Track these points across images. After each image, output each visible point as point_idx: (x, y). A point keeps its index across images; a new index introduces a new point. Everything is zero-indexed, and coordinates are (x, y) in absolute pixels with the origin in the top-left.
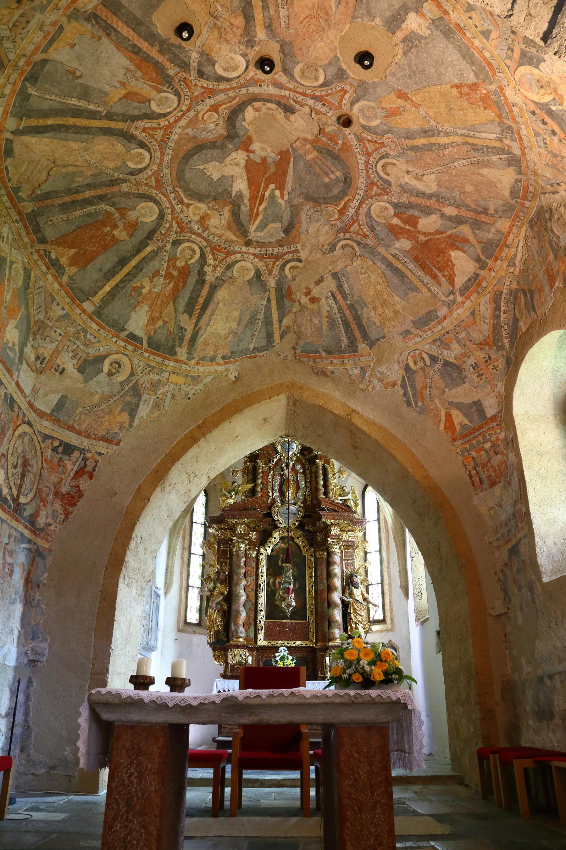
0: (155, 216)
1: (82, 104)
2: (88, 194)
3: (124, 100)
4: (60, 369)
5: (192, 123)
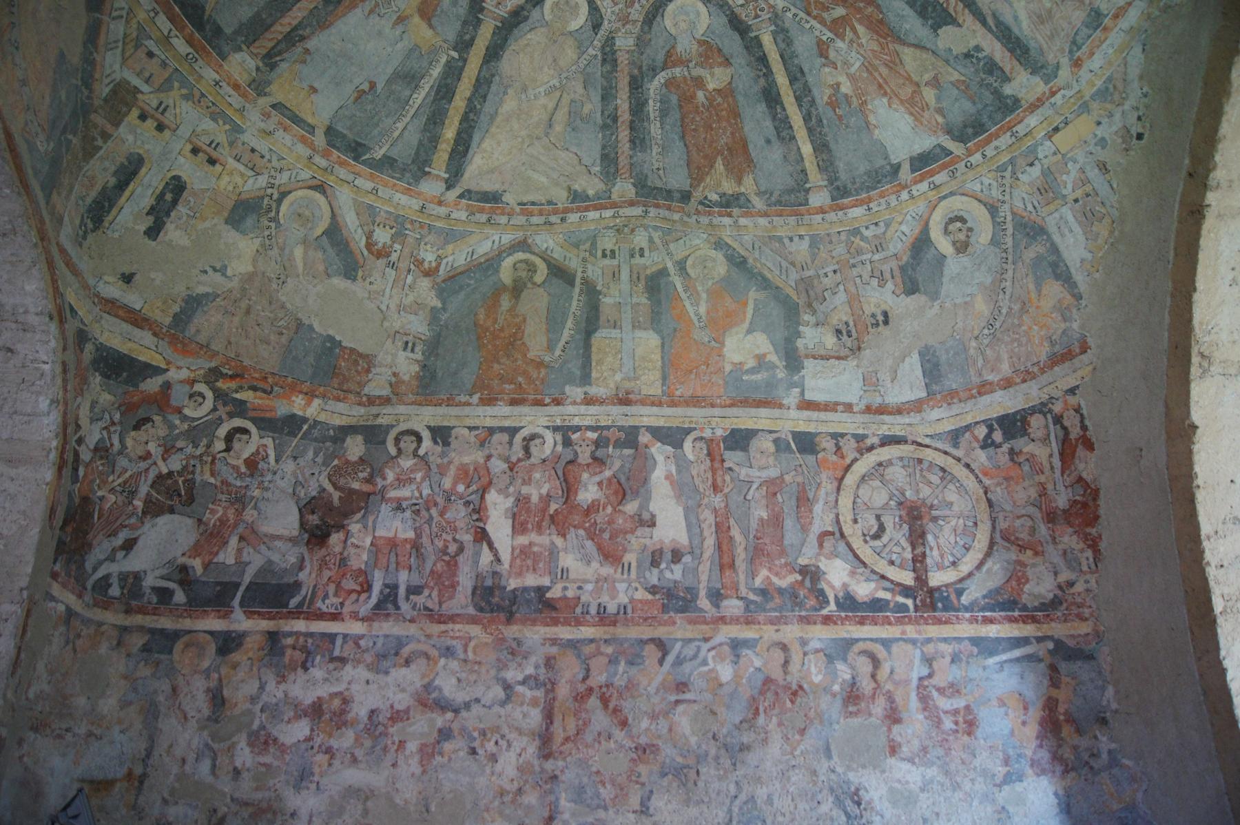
1: (426, 86)
2: (623, 102)
3: (434, 21)
4: (881, 318)
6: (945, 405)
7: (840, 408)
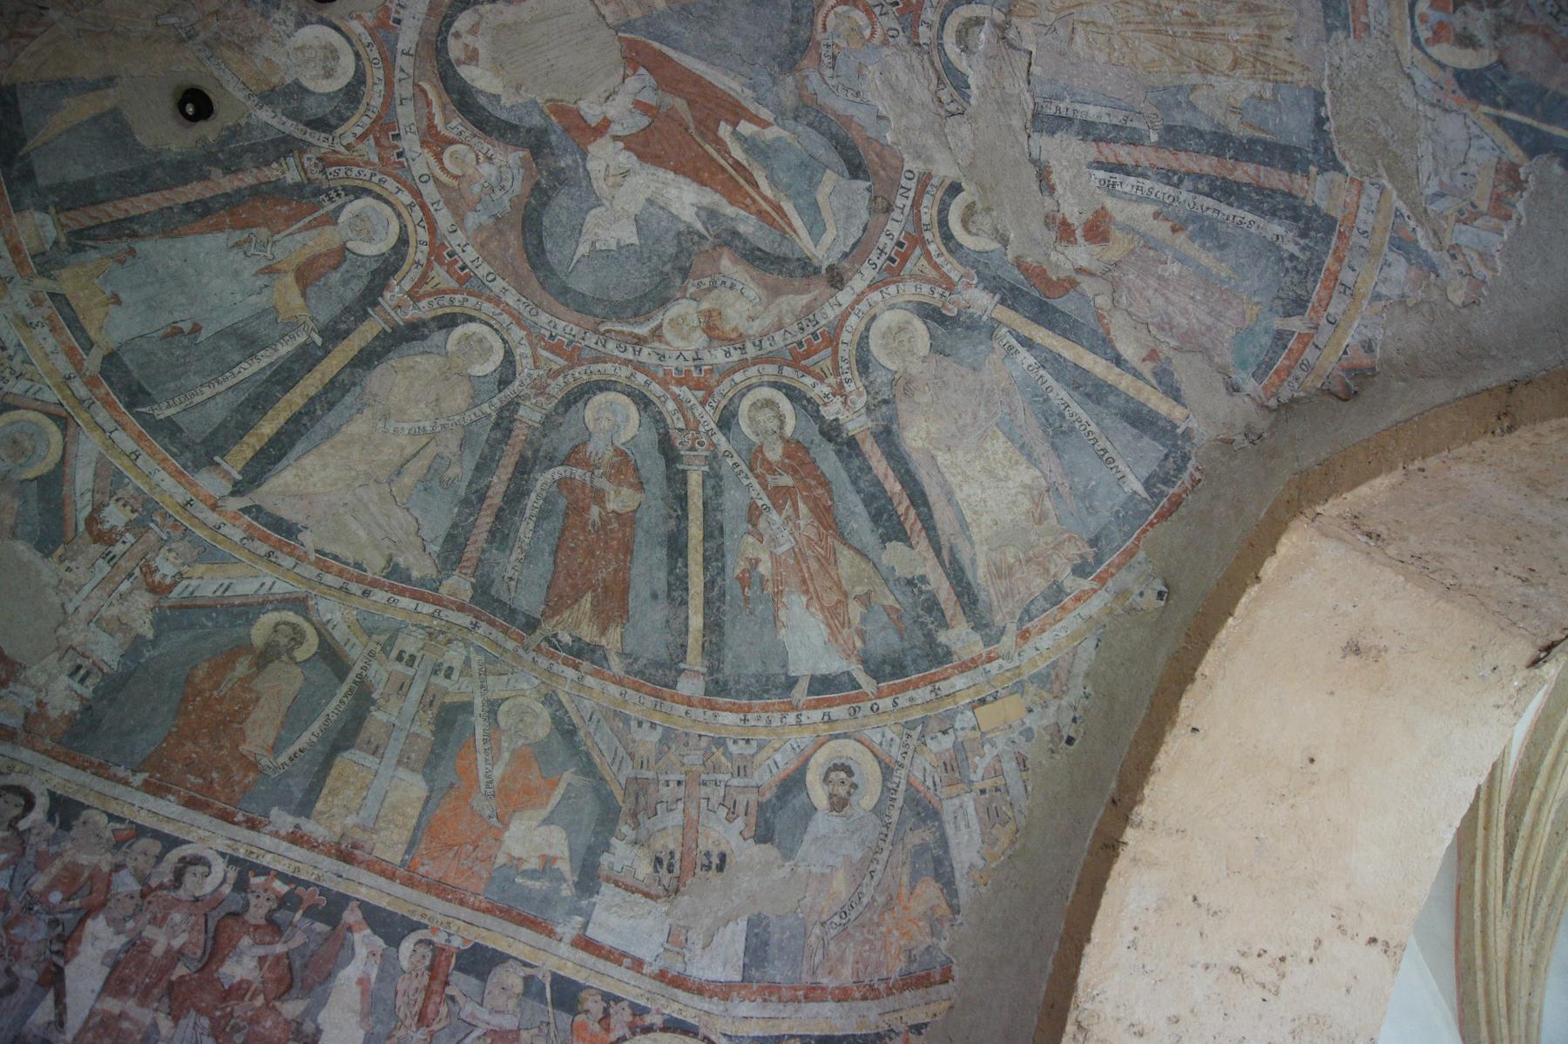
0: (633, 409)
1: (265, 359)
2: (499, 482)
3: (310, 291)
4: (715, 860)
5: (456, 202)
6: (759, 1000)
7: (627, 962)
